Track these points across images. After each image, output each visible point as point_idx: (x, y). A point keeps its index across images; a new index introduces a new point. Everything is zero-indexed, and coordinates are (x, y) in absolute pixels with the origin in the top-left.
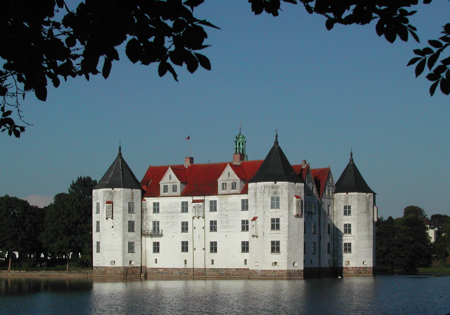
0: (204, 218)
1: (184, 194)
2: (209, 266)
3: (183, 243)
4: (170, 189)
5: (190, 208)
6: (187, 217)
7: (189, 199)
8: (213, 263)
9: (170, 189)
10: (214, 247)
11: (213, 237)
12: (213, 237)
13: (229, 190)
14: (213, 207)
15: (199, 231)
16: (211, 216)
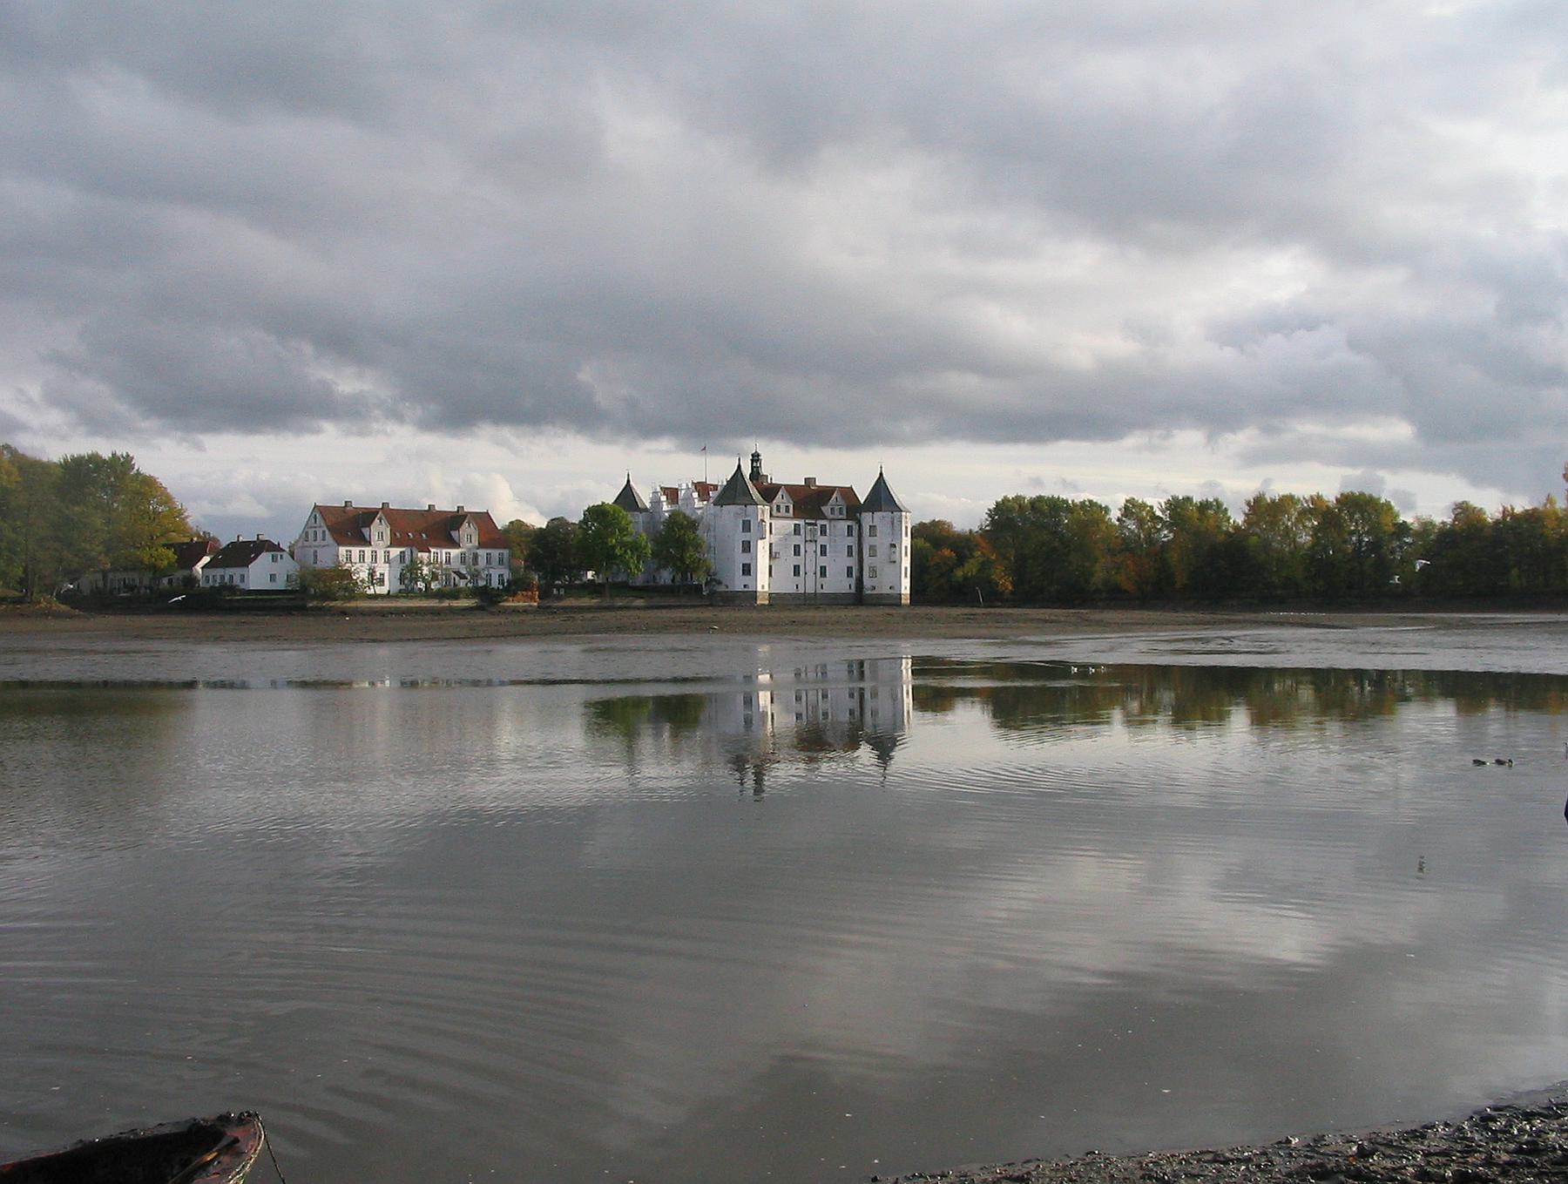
0: (816, 541)
1: (795, 516)
2: (820, 591)
3: (795, 566)
4: (783, 509)
5: (802, 531)
6: (798, 540)
7: (801, 522)
8: (822, 588)
9: (783, 509)
10: (823, 573)
11: (822, 561)
12: (822, 561)
13: (837, 515)
14: (823, 532)
15: (810, 554)
16: (822, 540)
